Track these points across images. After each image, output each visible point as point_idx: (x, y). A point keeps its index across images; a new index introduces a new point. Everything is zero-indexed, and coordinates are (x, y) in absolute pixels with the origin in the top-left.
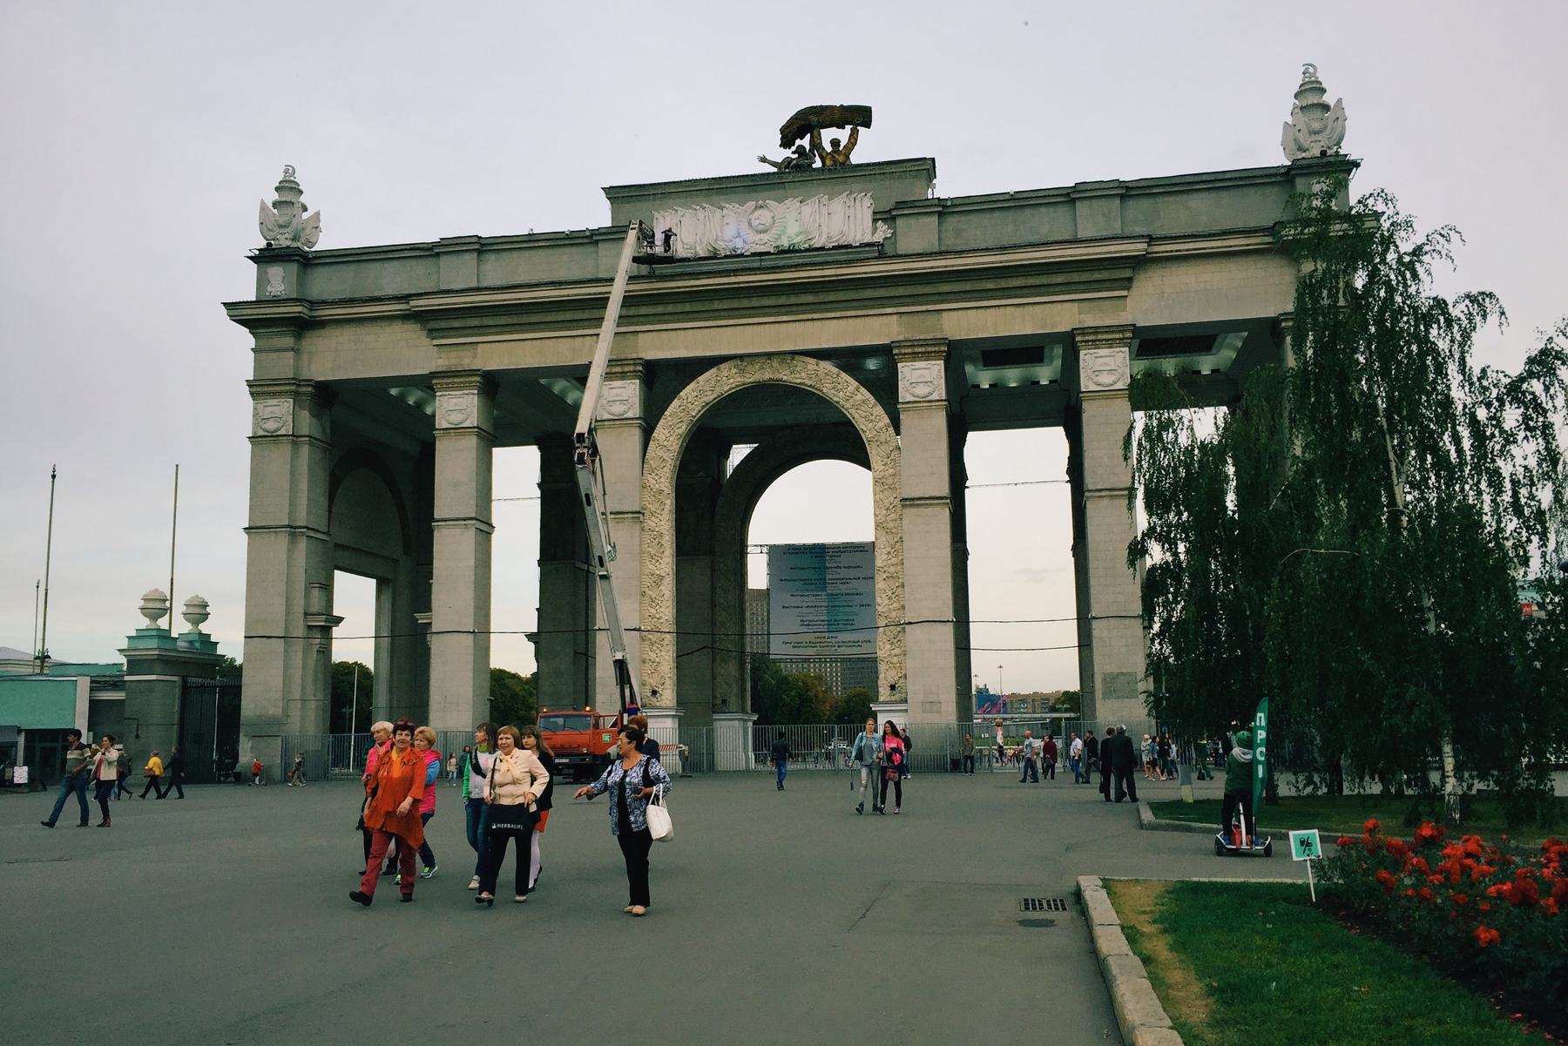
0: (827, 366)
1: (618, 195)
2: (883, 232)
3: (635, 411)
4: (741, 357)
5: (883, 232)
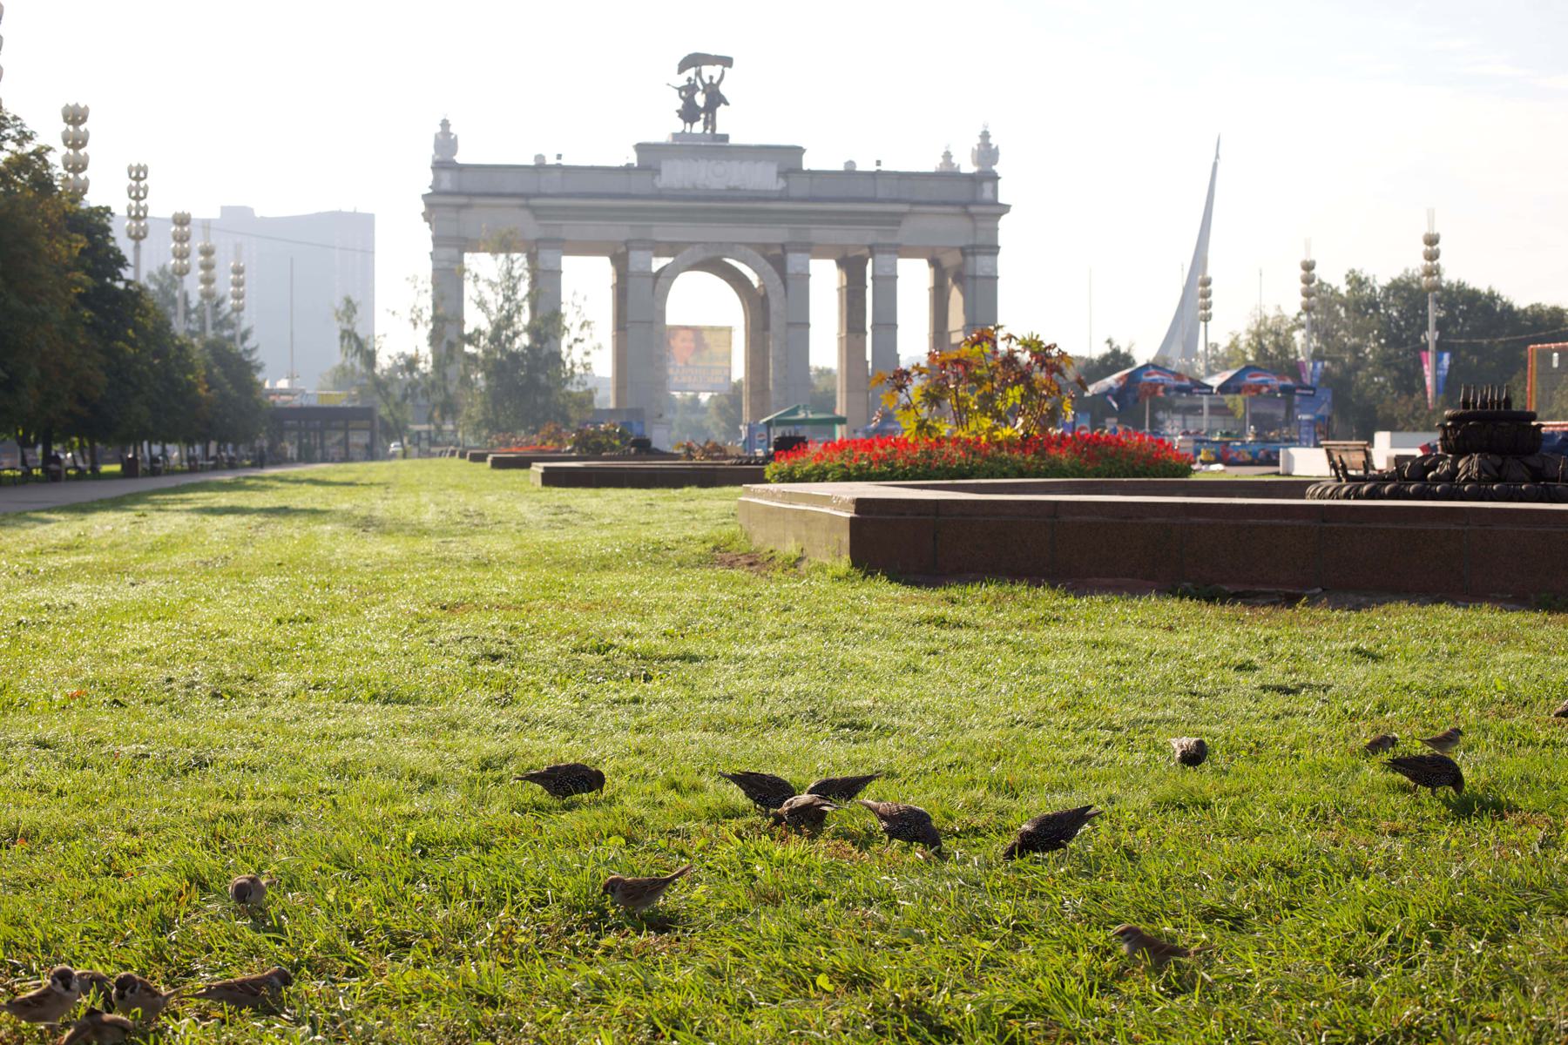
1: (641, 148)
2: (782, 184)
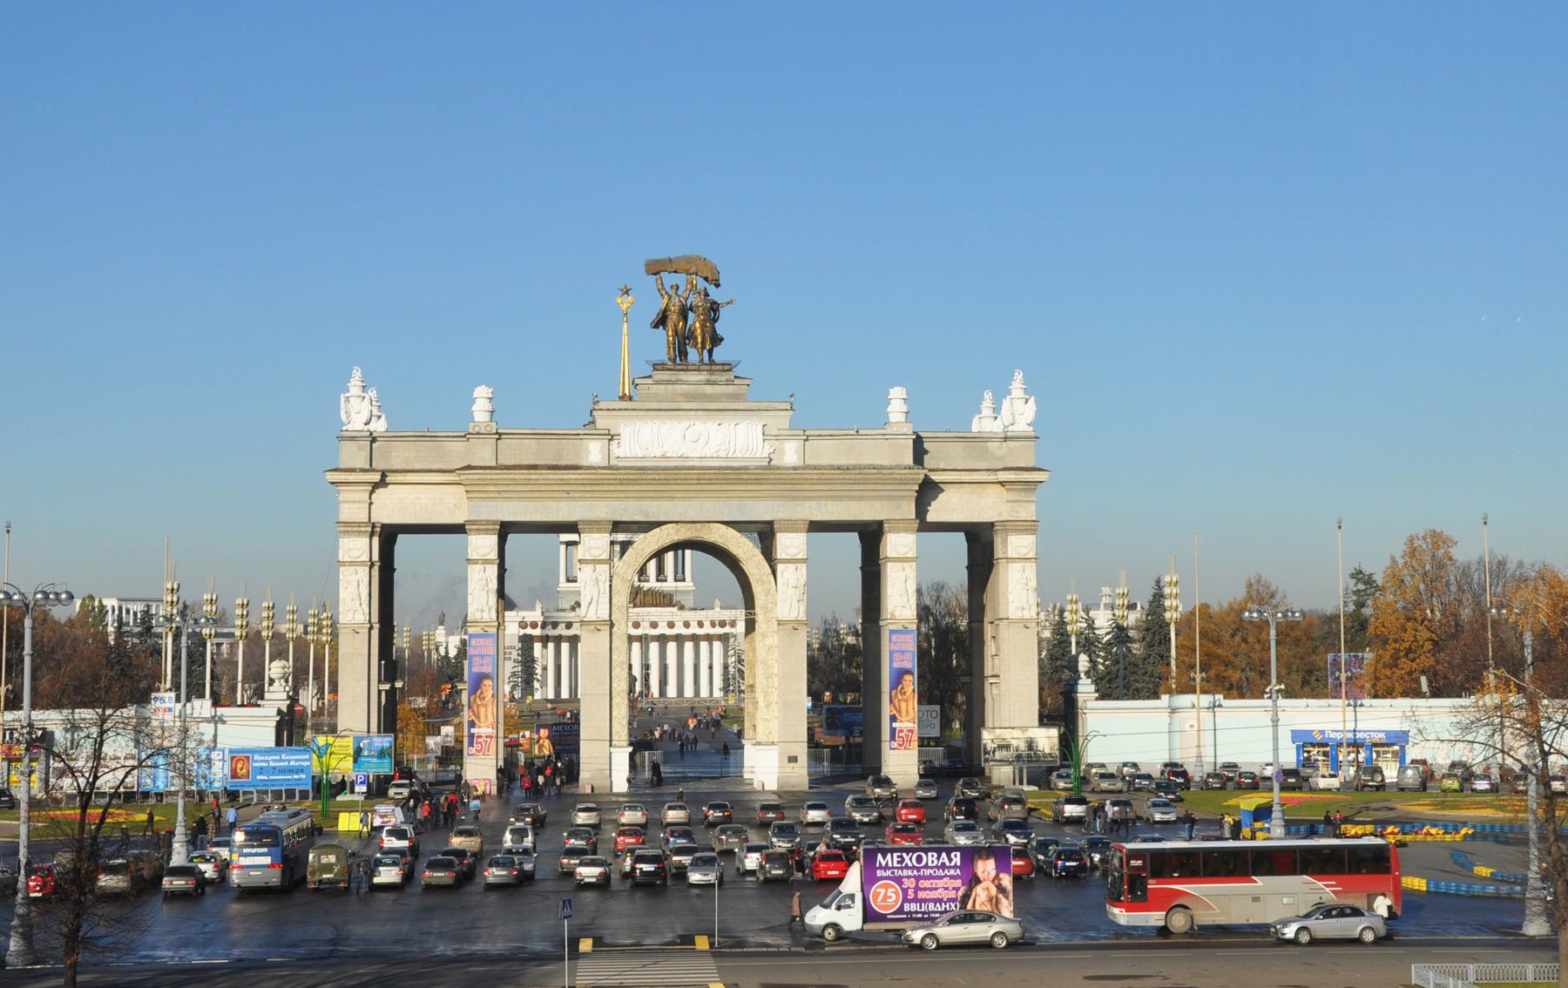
0: (732, 532)
5: (768, 449)
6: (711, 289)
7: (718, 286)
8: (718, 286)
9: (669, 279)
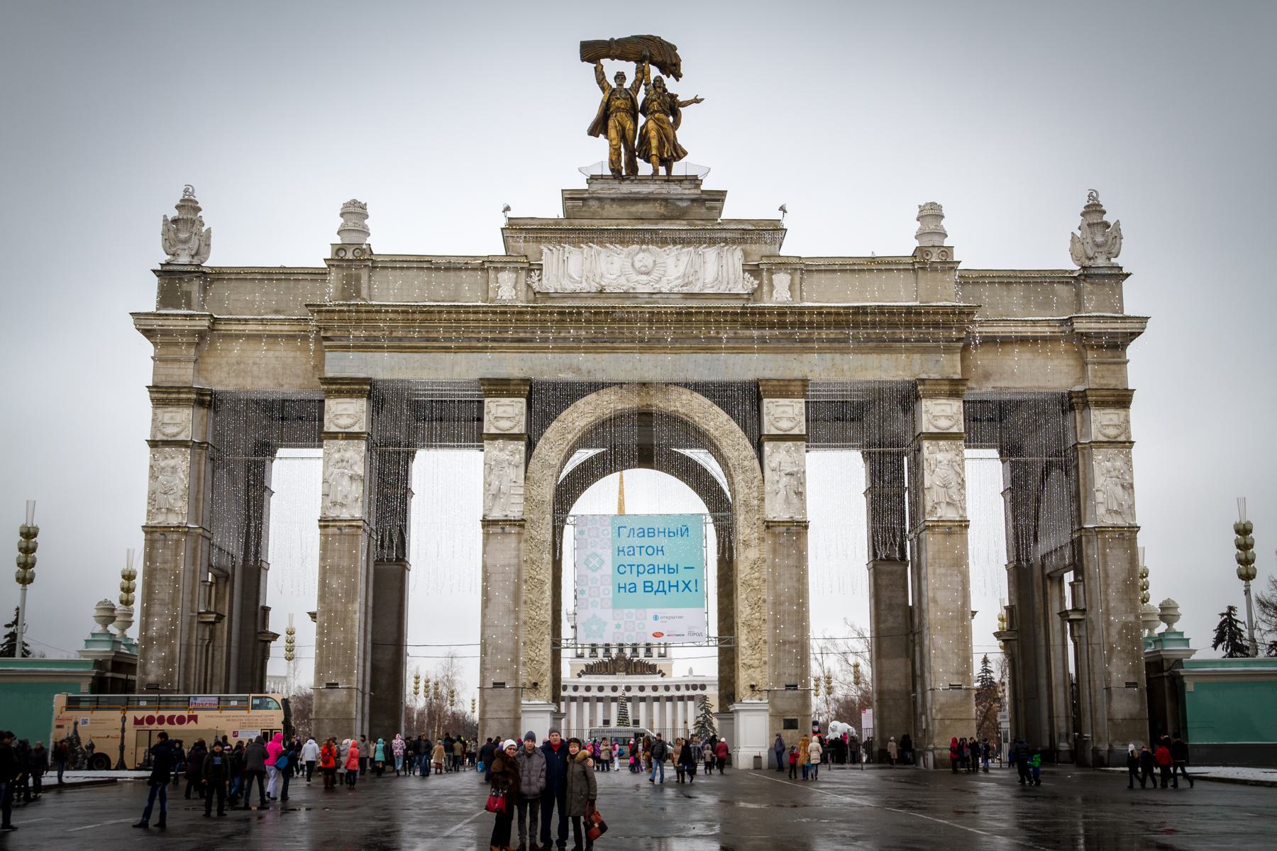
3: (521, 428)
4: (621, 384)
6: (670, 84)
7: (678, 76)
8: (678, 76)
9: (611, 67)
